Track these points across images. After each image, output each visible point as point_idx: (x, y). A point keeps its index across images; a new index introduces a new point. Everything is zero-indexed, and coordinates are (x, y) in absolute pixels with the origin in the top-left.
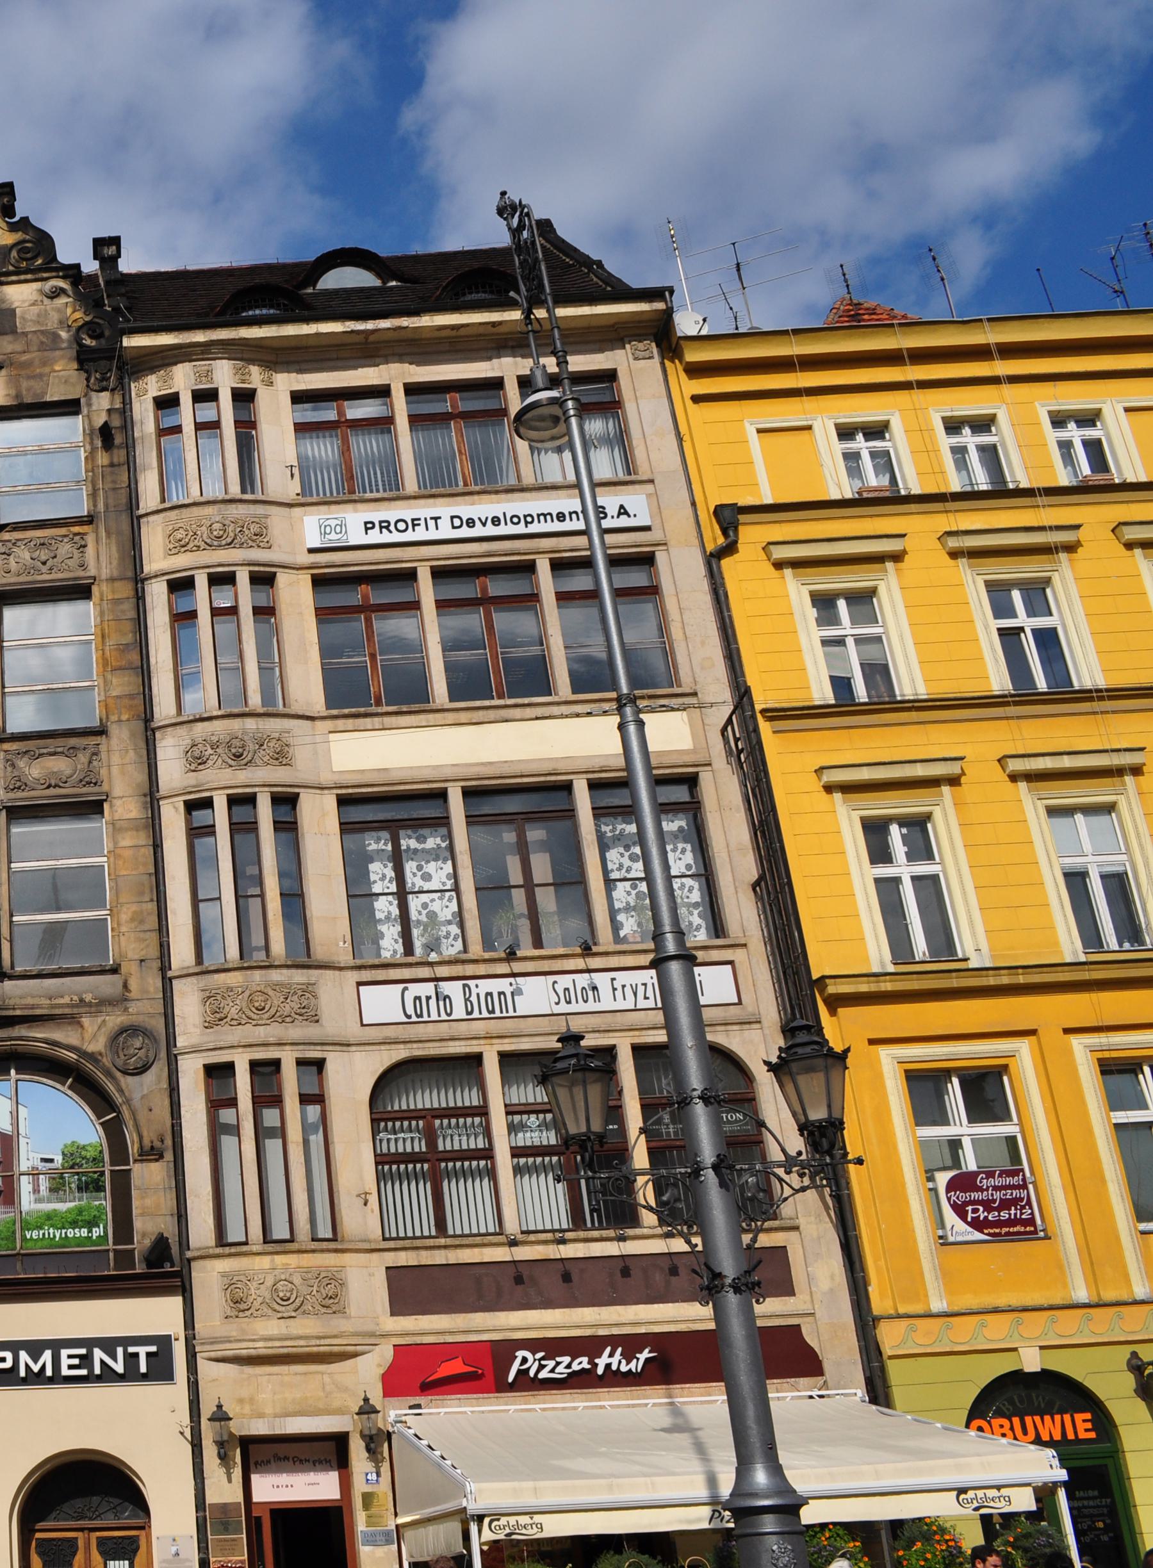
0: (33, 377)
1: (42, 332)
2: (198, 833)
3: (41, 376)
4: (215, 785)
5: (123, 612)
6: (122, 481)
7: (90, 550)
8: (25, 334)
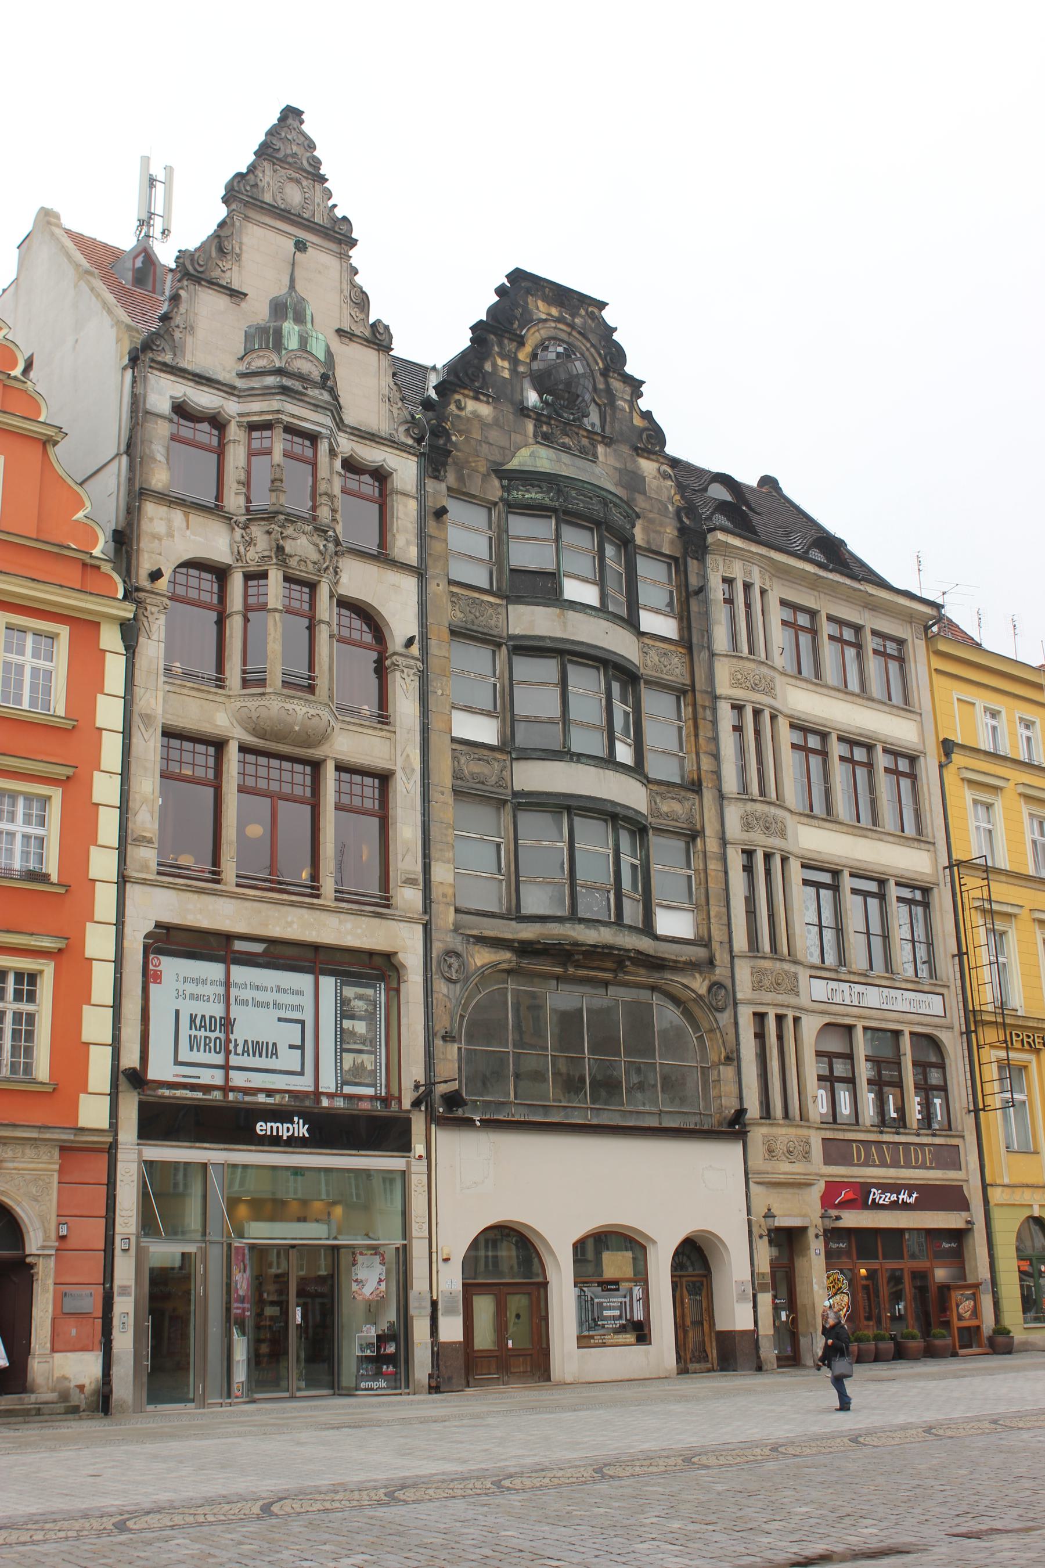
2: (749, 869)
4: (759, 843)
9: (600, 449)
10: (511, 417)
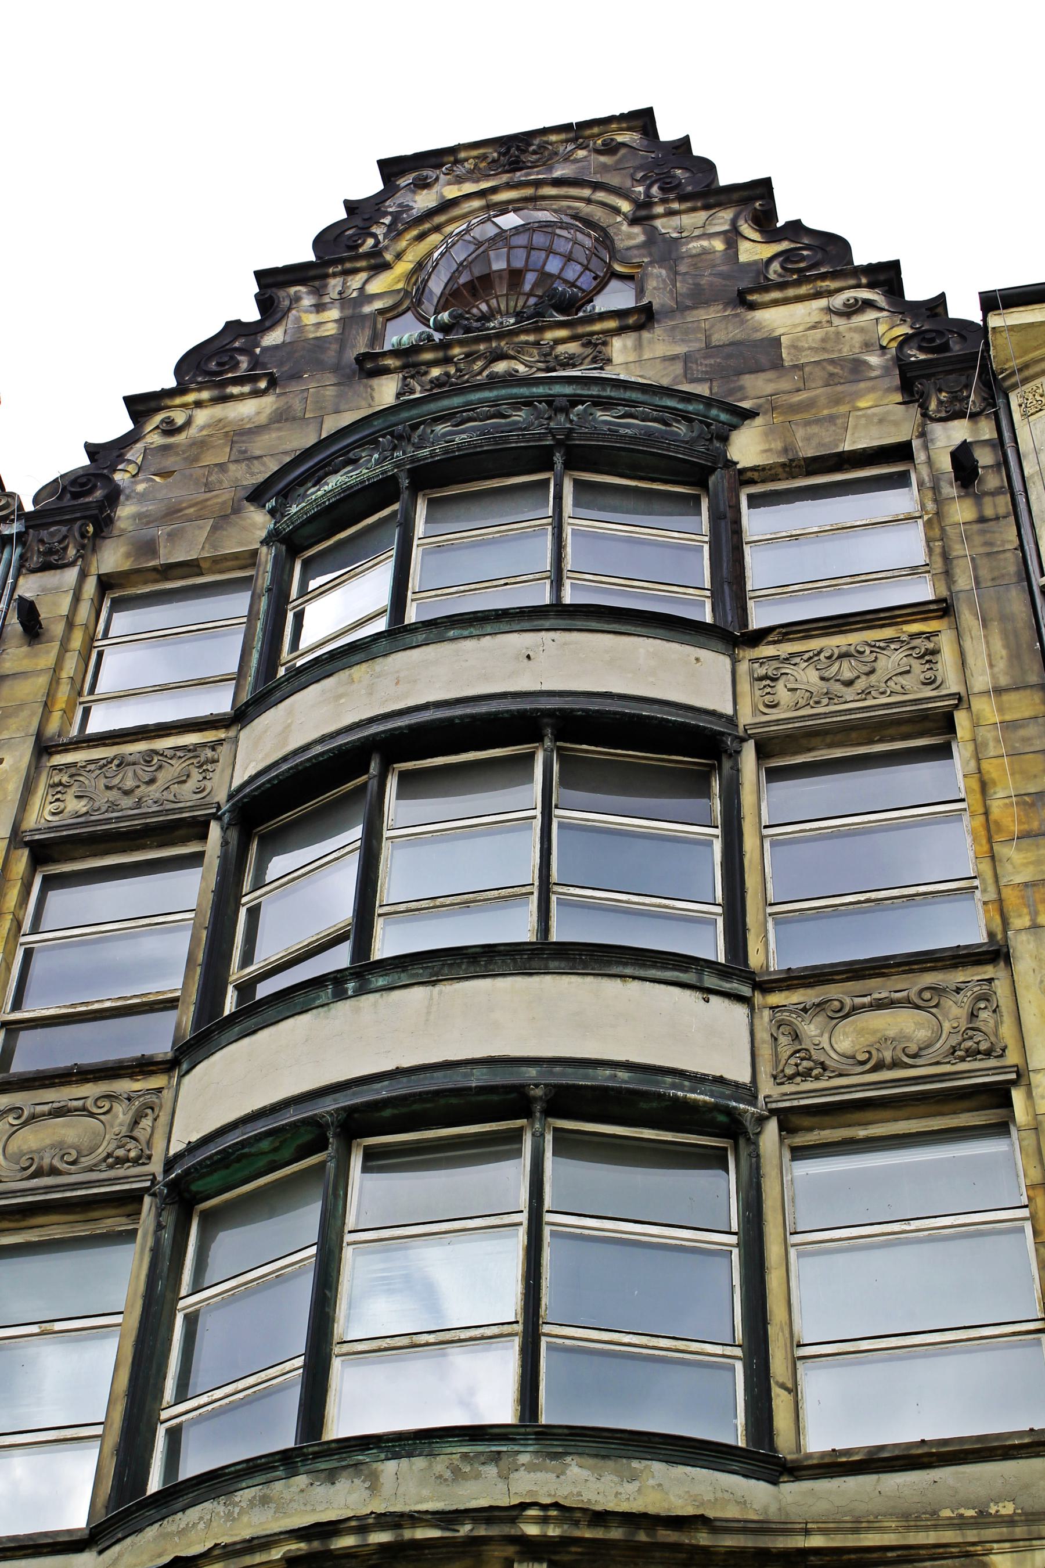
0: (818, 421)
1: (832, 361)
3: (832, 419)
5: (1025, 740)
6: (1004, 542)
7: (948, 657)
8: (800, 367)
9: (620, 348)
10: (331, 392)
